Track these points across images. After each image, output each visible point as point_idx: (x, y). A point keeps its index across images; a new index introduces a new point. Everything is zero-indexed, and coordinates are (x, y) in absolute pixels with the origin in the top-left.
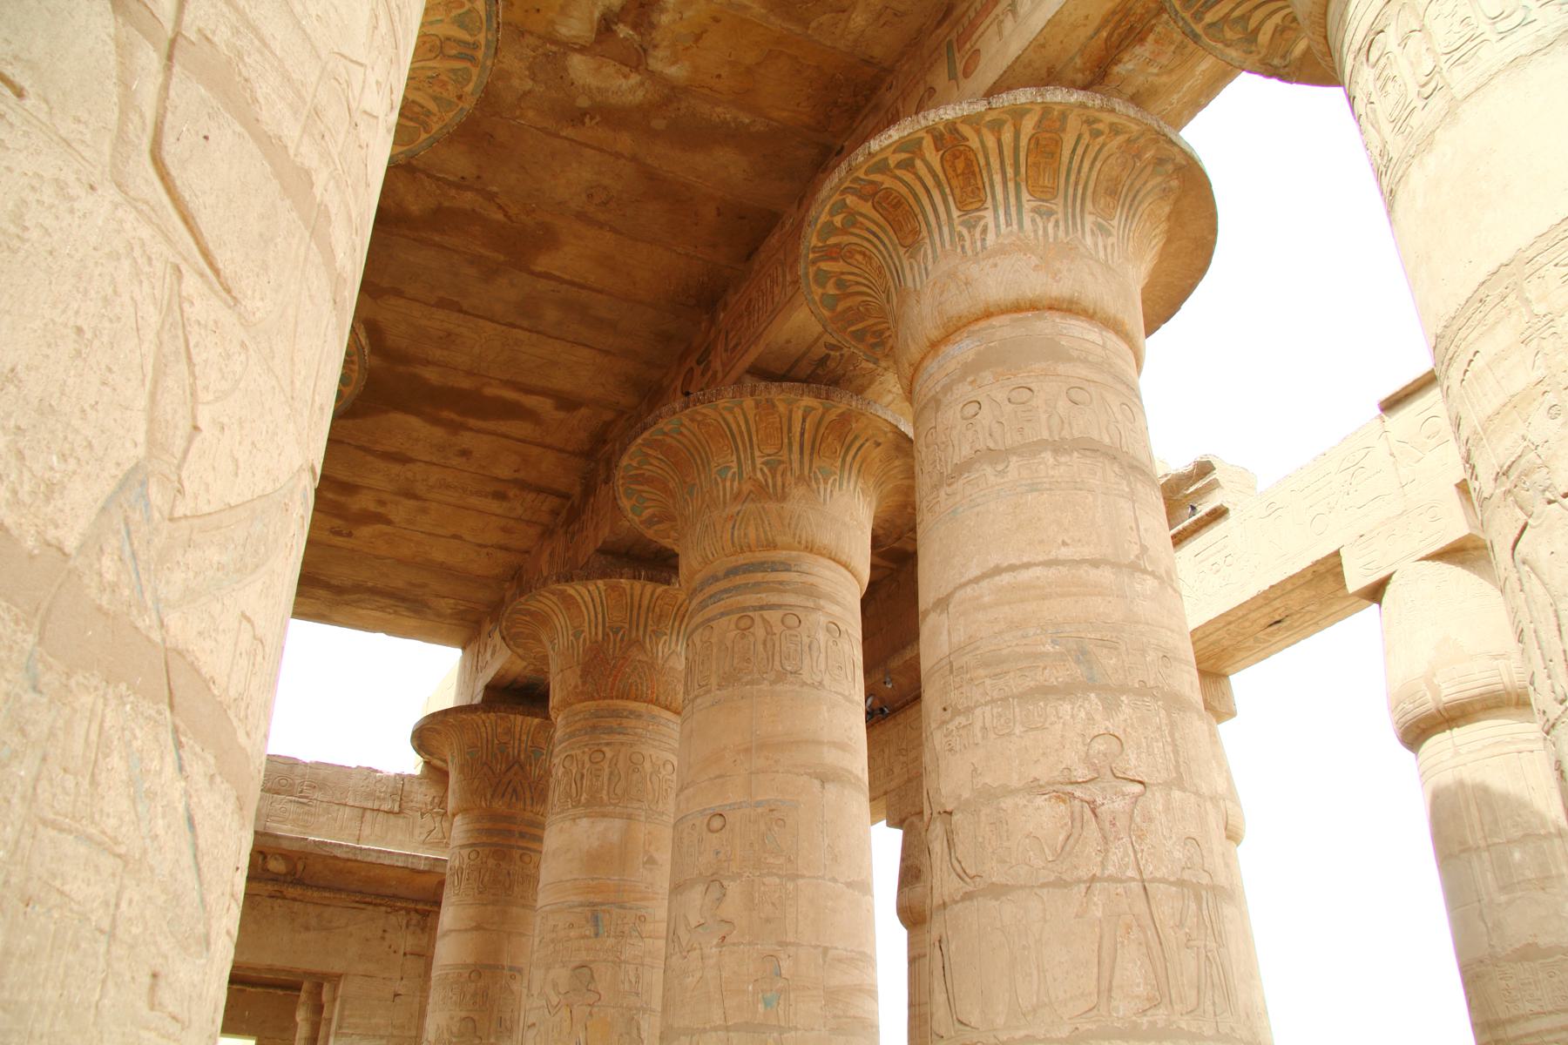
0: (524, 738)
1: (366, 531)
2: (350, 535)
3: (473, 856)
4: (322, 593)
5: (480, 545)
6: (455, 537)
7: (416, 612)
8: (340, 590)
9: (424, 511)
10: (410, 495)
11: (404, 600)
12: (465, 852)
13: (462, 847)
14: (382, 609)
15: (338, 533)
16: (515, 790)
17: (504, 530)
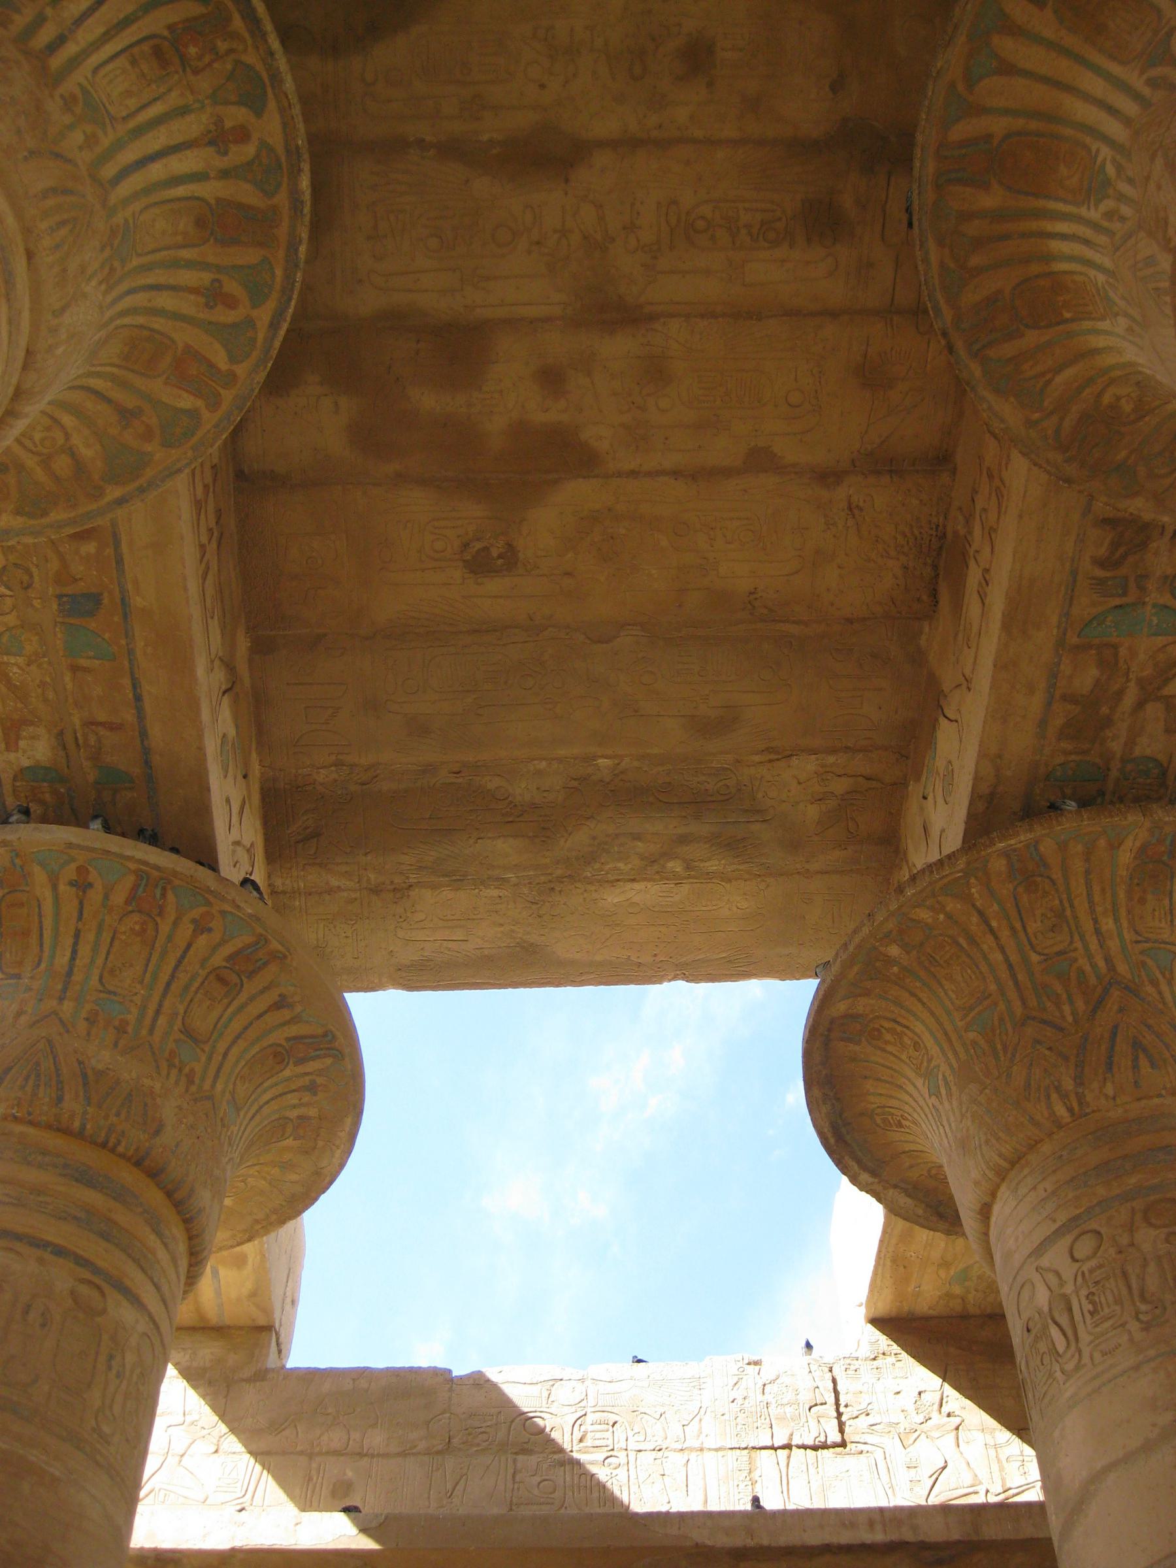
0: (1108, 924)
1: (545, 524)
2: (510, 560)
3: (1085, 1247)
4: (505, 849)
5: (828, 477)
6: (760, 460)
7: (733, 846)
8: (539, 822)
9: (655, 372)
10: (611, 312)
11: (697, 803)
12: (1056, 1257)
13: (1039, 1250)
14: (652, 867)
15: (480, 565)
16: (1137, 1045)
17: (871, 376)
